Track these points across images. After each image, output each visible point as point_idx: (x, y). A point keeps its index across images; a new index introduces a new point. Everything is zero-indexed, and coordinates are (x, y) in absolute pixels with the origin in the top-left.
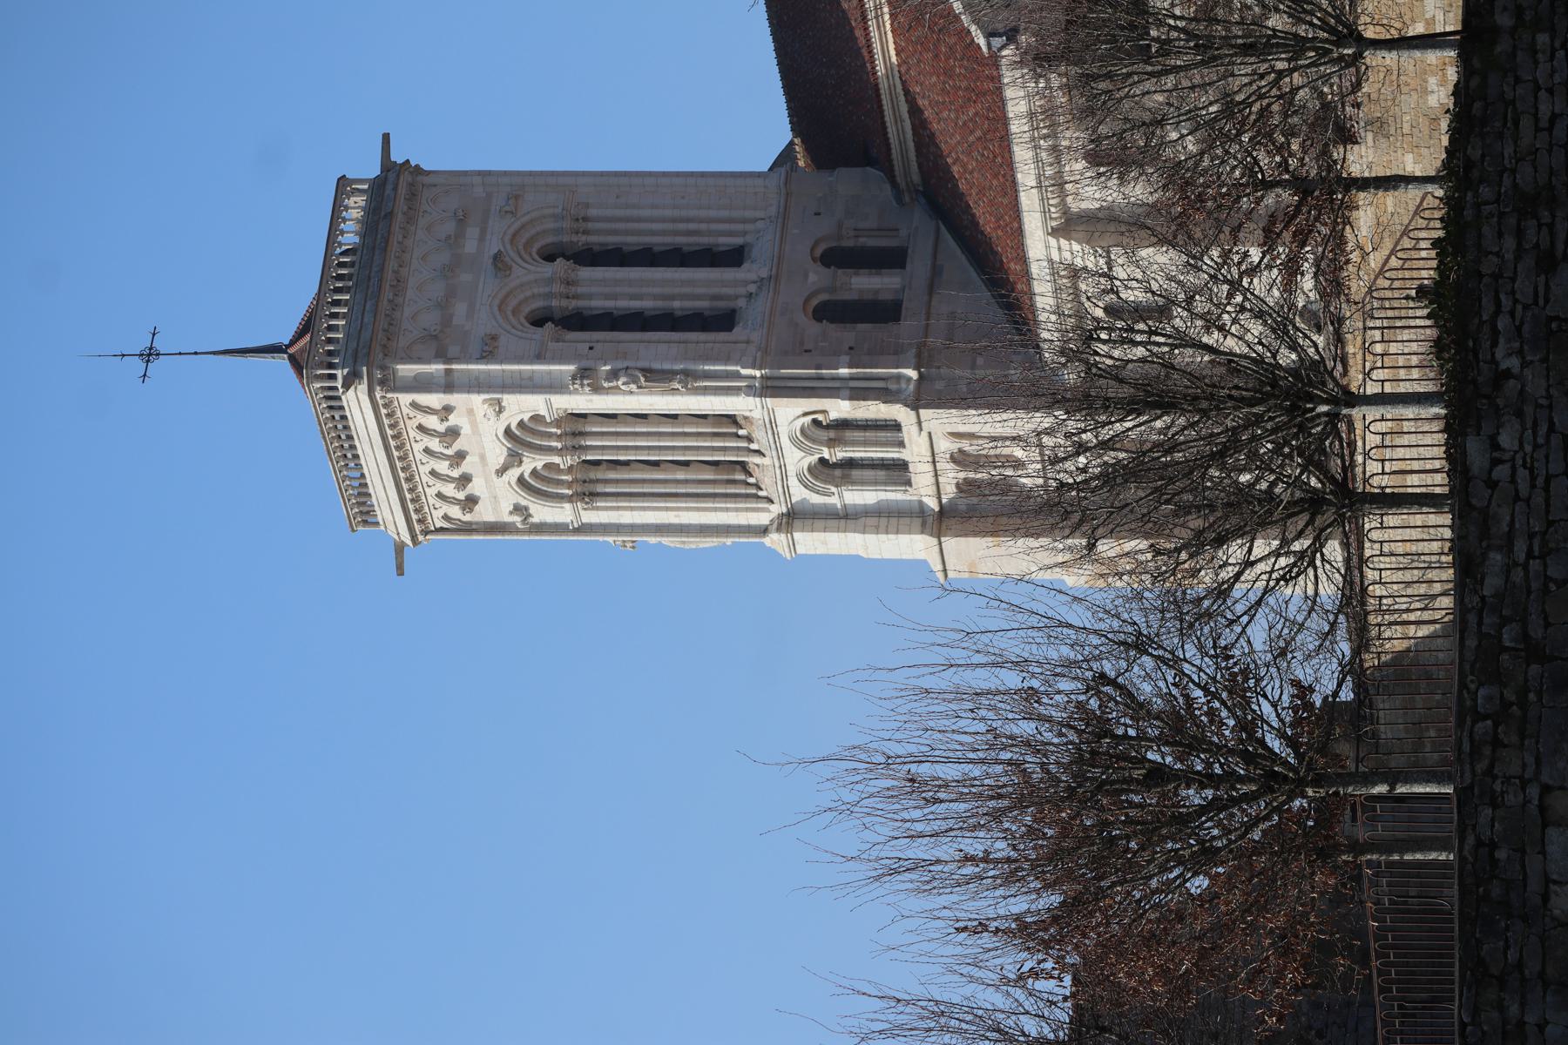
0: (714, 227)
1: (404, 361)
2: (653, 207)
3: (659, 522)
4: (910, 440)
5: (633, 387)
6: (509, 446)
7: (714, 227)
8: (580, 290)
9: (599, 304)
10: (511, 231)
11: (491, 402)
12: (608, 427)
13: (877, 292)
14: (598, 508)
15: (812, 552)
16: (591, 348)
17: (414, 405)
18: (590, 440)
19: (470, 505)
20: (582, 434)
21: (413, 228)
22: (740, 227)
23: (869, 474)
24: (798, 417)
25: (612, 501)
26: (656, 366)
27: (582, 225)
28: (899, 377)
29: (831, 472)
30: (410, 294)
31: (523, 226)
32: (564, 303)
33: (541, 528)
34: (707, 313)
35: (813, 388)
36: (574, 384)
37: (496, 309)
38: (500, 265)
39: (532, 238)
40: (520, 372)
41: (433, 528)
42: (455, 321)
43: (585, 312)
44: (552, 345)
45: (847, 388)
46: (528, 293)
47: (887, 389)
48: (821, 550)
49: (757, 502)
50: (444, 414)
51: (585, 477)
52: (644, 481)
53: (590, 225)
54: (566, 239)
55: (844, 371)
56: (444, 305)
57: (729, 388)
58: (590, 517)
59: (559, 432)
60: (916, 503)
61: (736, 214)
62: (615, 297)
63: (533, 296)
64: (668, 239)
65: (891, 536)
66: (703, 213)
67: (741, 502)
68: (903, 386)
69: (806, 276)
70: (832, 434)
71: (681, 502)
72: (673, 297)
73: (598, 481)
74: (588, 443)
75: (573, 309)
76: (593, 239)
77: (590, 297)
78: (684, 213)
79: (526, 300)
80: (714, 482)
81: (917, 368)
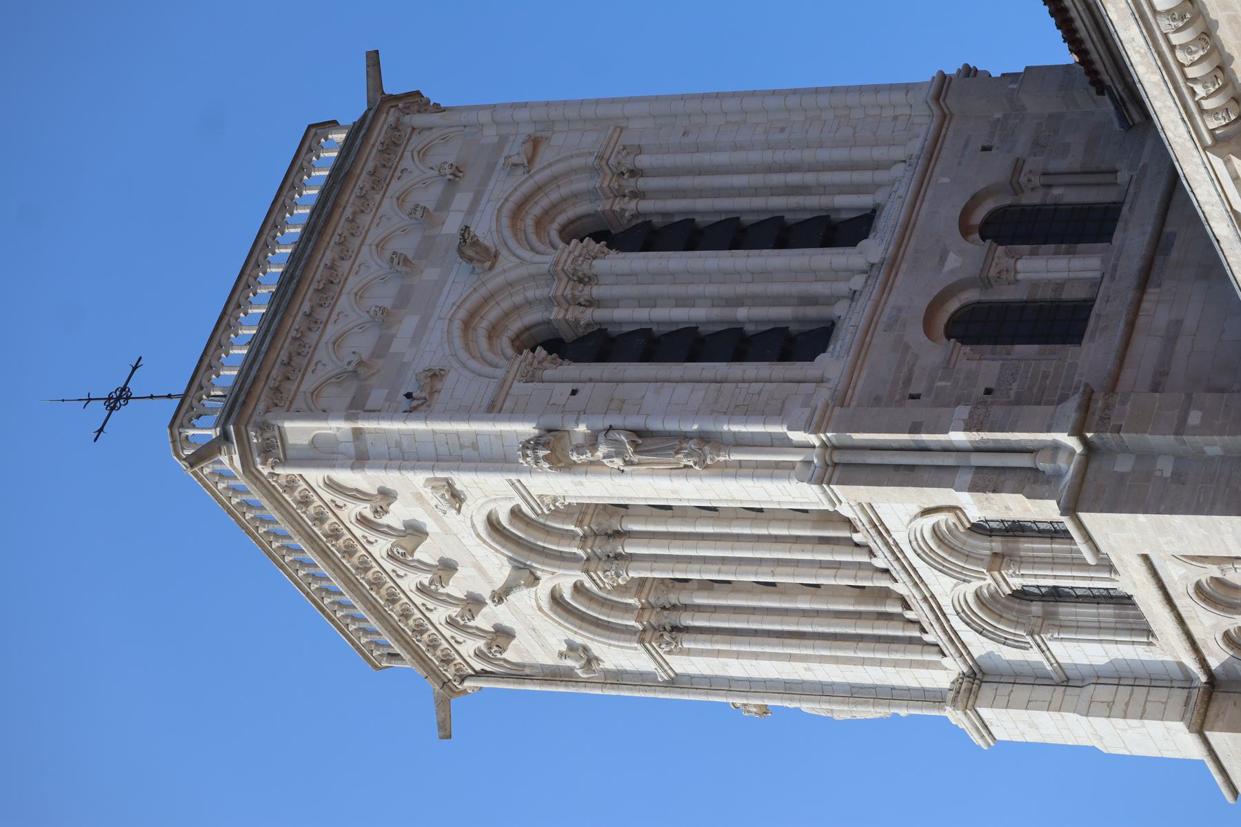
0: (827, 177)
1: (300, 414)
2: (737, 147)
3: (785, 677)
4: (1121, 560)
5: (618, 462)
6: (510, 555)
7: (827, 177)
8: (597, 291)
9: (627, 315)
10: (517, 196)
11: (433, 484)
12: (656, 524)
13: (1060, 285)
14: (689, 652)
15: (1020, 739)
16: (574, 392)
17: (332, 485)
18: (631, 545)
19: (500, 641)
20: (618, 534)
21: (378, 197)
22: (865, 177)
23: (1087, 612)
24: (916, 517)
25: (705, 641)
26: (655, 425)
27: (630, 184)
28: (1056, 447)
29: (1024, 608)
30: (344, 303)
31: (540, 188)
32: (573, 313)
33: (618, 678)
34: (794, 328)
35: (911, 468)
36: (525, 456)
37: (457, 324)
38: (470, 252)
39: (554, 206)
40: (458, 434)
41: (470, 672)
42: (395, 347)
43: (610, 329)
44: (519, 387)
45: (971, 467)
46: (518, 299)
47: (1036, 470)
48: (1032, 737)
49: (922, 653)
50: (379, 502)
51: (662, 601)
52: (753, 610)
53: (642, 183)
54: (603, 206)
55: (958, 437)
56: (384, 318)
57: (777, 465)
58: (682, 665)
59: (579, 531)
60: (1176, 667)
61: (860, 154)
62: (652, 302)
63: (529, 303)
64: (758, 202)
65: (1129, 721)
66: (808, 155)
67: (897, 651)
68: (1062, 463)
69: (943, 259)
70: (997, 545)
71: (806, 647)
72: (737, 301)
73: (686, 607)
74: (629, 550)
75: (588, 325)
76: (646, 205)
77: (615, 303)
78: (780, 156)
79: (517, 308)
80: (858, 615)
81: (1078, 432)
